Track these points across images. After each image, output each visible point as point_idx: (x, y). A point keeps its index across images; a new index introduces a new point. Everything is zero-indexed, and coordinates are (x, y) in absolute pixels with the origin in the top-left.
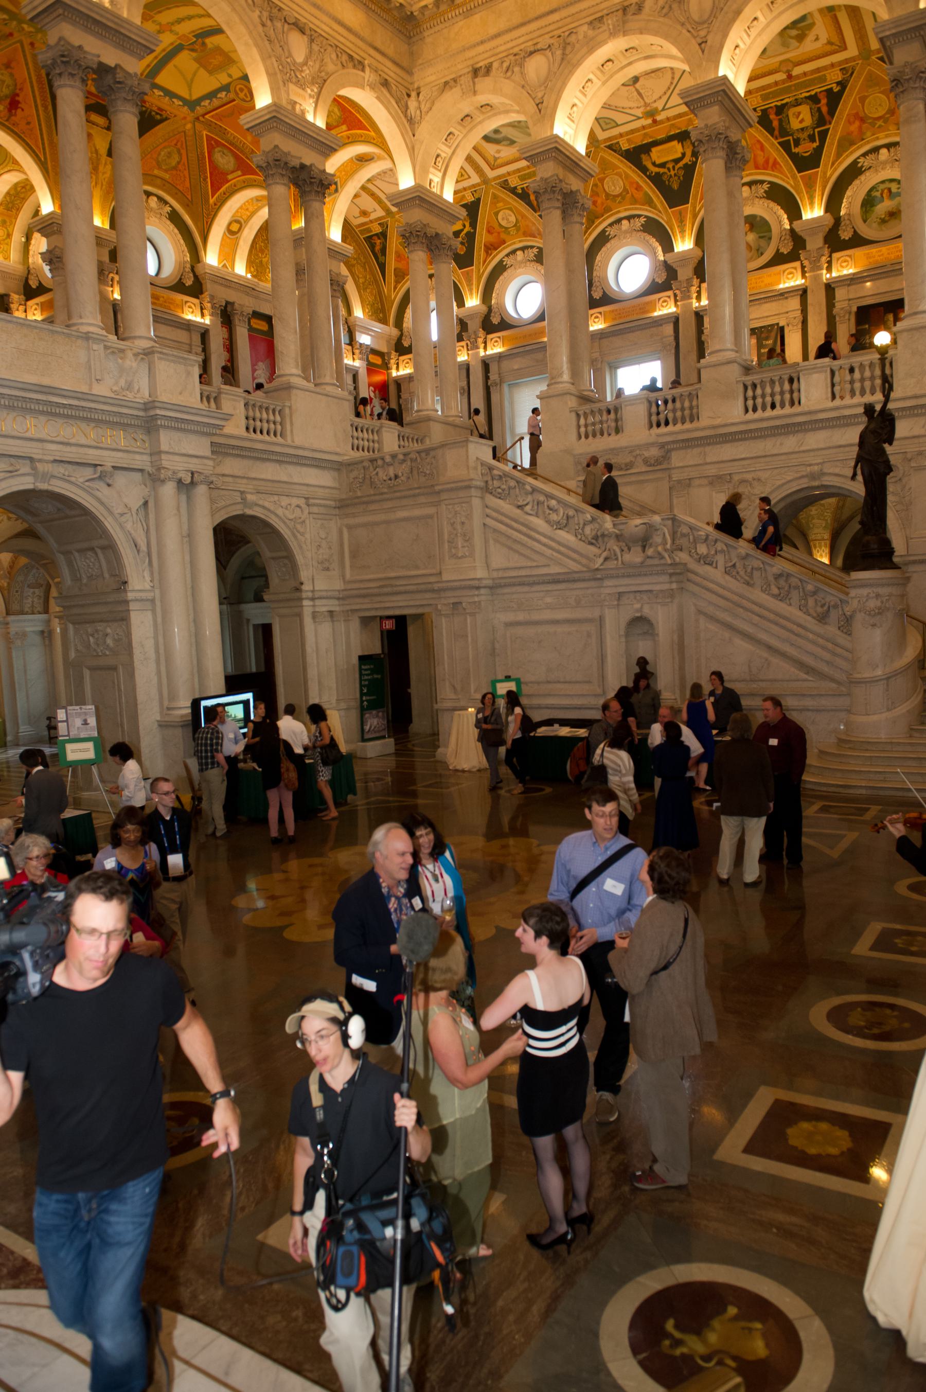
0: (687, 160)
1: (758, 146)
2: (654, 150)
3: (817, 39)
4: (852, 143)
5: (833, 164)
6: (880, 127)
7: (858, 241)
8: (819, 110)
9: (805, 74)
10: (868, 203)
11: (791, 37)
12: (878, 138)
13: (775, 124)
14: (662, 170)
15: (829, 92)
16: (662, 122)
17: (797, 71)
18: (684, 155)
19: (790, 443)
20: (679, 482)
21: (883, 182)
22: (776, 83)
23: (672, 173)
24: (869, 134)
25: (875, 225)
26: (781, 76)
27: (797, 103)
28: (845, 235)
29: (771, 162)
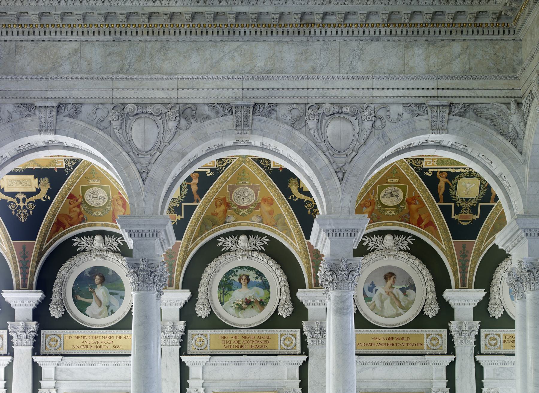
0: (41, 196)
1: (121, 203)
4: (215, 224)
5: (195, 239)
6: (243, 215)
7: (214, 322)
10: (226, 286)
12: (240, 225)
14: (10, 199)
18: (38, 191)
21: (242, 268)
23: (22, 204)
24: (232, 219)
25: (232, 310)
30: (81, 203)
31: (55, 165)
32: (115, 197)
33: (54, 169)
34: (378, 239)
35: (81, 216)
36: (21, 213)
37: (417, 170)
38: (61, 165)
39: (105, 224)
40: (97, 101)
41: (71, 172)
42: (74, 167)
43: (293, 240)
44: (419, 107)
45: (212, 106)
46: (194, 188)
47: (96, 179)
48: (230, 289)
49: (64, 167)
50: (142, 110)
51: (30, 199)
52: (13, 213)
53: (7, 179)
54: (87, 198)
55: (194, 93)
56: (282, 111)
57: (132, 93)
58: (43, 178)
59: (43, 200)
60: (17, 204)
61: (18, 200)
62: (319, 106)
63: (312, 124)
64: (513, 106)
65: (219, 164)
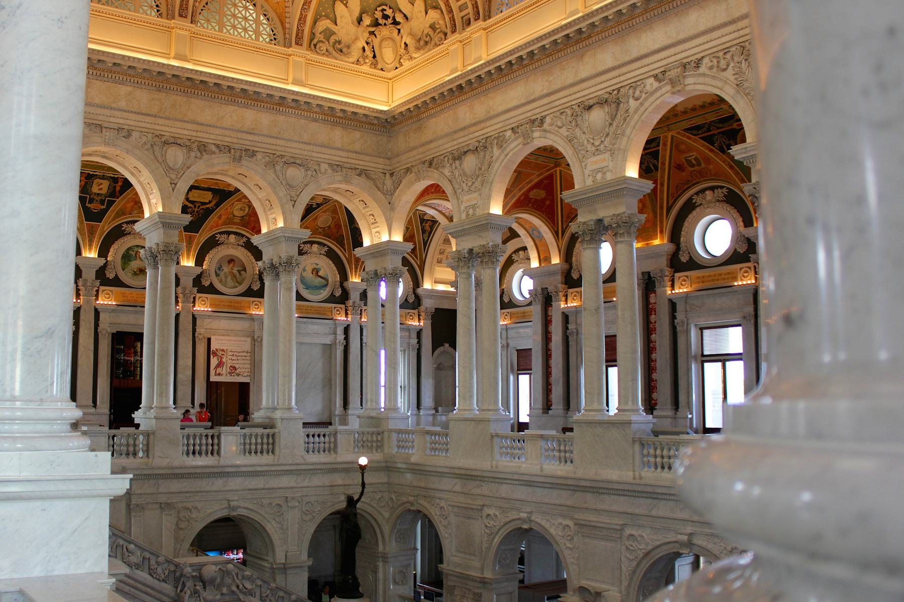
4: (124, 214)
7: (117, 282)
19: (218, 484)
20: (137, 505)
25: (130, 275)
27: (103, 178)
28: (111, 275)
34: (226, 236)
40: (143, 130)
44: (337, 167)
45: (217, 146)
46: (118, 189)
48: (129, 260)
50: (175, 142)
55: (207, 136)
56: (259, 156)
57: (167, 129)
62: (282, 156)
63: (278, 168)
64: (388, 176)
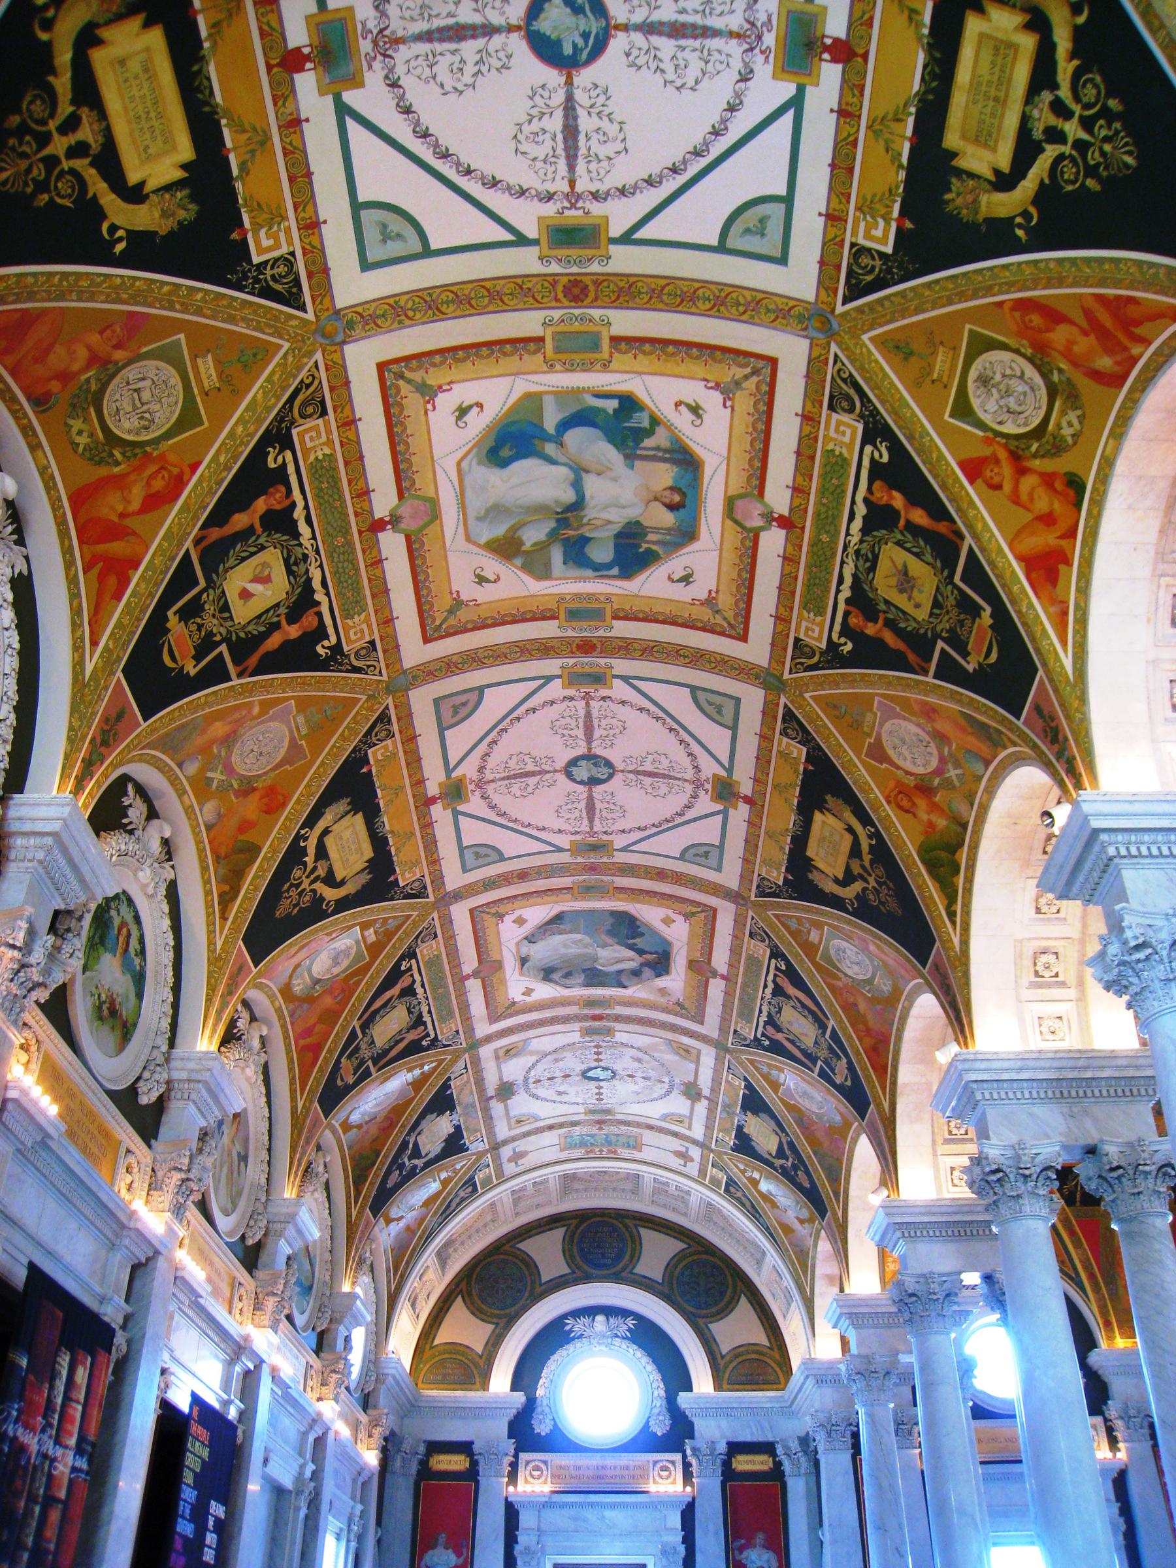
0: (122, 216)
1: (158, 484)
2: (156, 38)
3: (481, 580)
8: (274, 627)
9: (377, 563)
11: (515, 529)
12: (181, 793)
13: (240, 521)
15: (320, 633)
16: (284, 94)
17: (392, 544)
18: (135, 195)
22: (364, 494)
26: (384, 502)
29: (117, 548)
30: (108, 362)
31: (257, 227)
32: (172, 458)
33: (241, 223)
35: (55, 386)
36: (24, 155)
37: (410, 947)
38: (263, 246)
39: (52, 477)
41: (241, 289)
42: (267, 293)
43: (224, 918)
47: (220, 375)
49: (256, 260)
51: (91, 175)
52: (15, 120)
53: (147, 50)
54: (131, 373)
58: (193, 198)
59: (105, 226)
60: (52, 125)
61: (71, 124)
65: (356, 653)
